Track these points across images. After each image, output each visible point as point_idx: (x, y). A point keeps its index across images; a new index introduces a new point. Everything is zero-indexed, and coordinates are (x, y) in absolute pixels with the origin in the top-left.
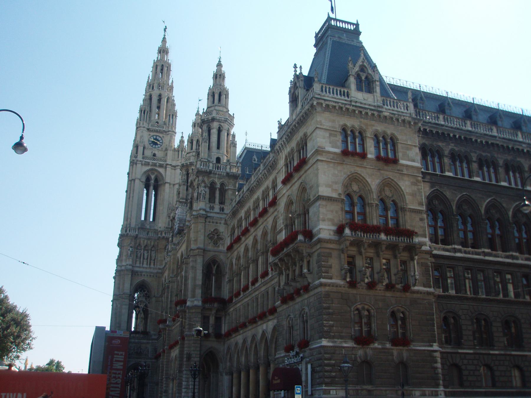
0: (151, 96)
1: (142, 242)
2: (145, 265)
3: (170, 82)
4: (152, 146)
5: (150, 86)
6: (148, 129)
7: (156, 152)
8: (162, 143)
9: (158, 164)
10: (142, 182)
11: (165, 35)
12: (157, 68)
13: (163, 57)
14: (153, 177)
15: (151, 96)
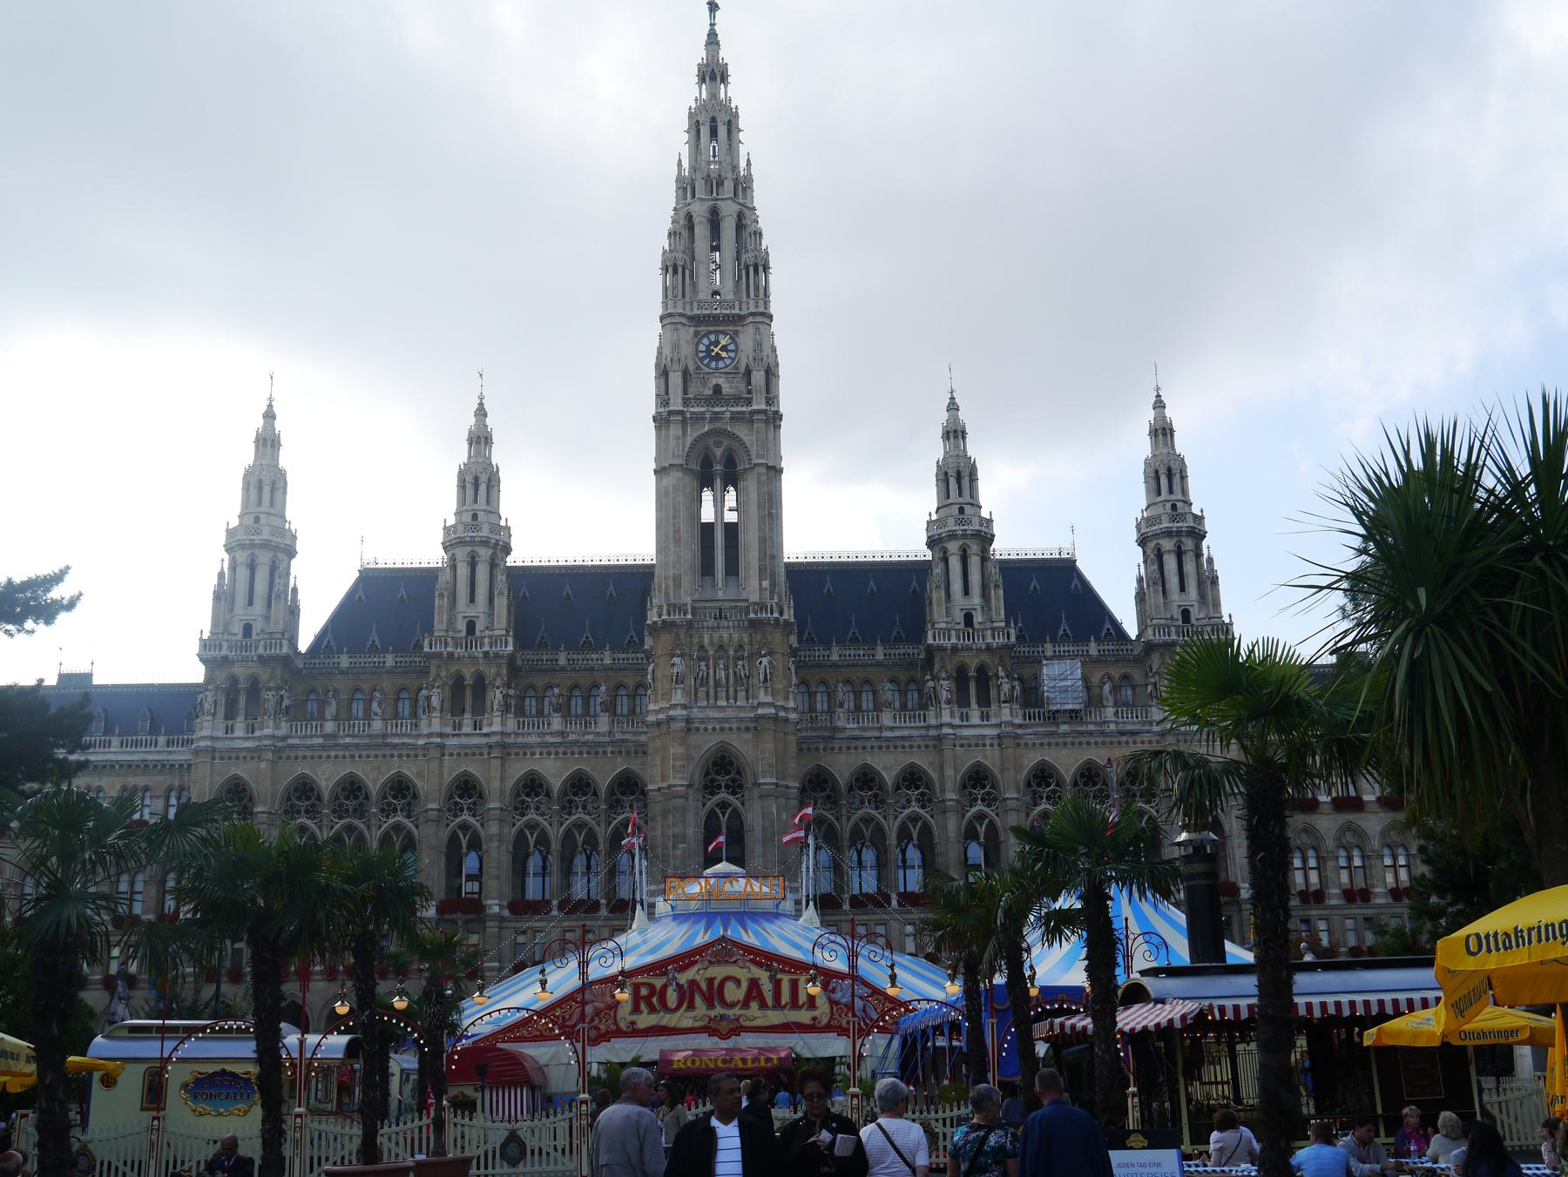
0: (689, 217)
1: (706, 641)
2: (723, 703)
3: (743, 164)
4: (707, 366)
5: (685, 187)
6: (691, 318)
7: (721, 381)
8: (736, 351)
9: (728, 415)
10: (692, 470)
11: (712, 25)
12: (698, 131)
13: (714, 95)
14: (718, 452)
15: (689, 217)
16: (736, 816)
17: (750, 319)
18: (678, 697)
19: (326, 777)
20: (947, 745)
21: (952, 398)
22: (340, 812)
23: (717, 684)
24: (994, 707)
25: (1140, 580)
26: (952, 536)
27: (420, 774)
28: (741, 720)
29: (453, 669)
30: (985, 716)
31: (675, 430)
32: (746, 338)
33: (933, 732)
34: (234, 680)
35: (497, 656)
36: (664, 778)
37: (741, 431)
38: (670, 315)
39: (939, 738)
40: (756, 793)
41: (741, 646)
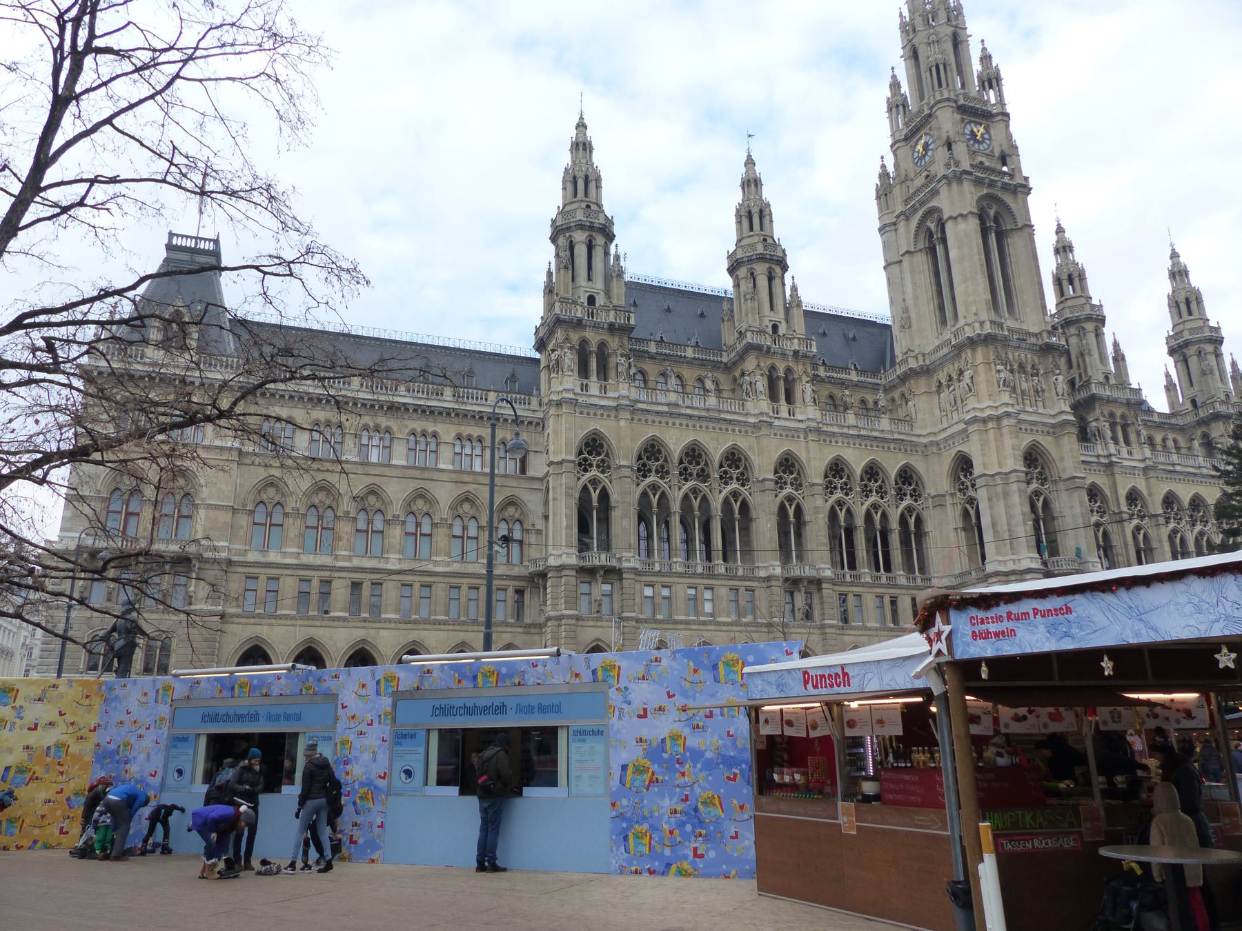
7: (984, 159)
8: (990, 139)
9: (999, 184)
14: (992, 213)
16: (1046, 504)
17: (1000, 118)
18: (1006, 398)
19: (676, 441)
20: (1117, 470)
21: (1059, 225)
22: (685, 475)
23: (1023, 392)
24: (1135, 446)
25: (1168, 375)
26: (1089, 318)
27: (750, 448)
28: (1045, 424)
29: (769, 362)
30: (1130, 453)
31: (967, 186)
32: (997, 131)
33: (1103, 460)
34: (584, 342)
35: (805, 356)
36: (1000, 465)
37: (1008, 198)
38: (948, 100)
39: (1111, 464)
40: (1061, 486)
41: (1033, 367)
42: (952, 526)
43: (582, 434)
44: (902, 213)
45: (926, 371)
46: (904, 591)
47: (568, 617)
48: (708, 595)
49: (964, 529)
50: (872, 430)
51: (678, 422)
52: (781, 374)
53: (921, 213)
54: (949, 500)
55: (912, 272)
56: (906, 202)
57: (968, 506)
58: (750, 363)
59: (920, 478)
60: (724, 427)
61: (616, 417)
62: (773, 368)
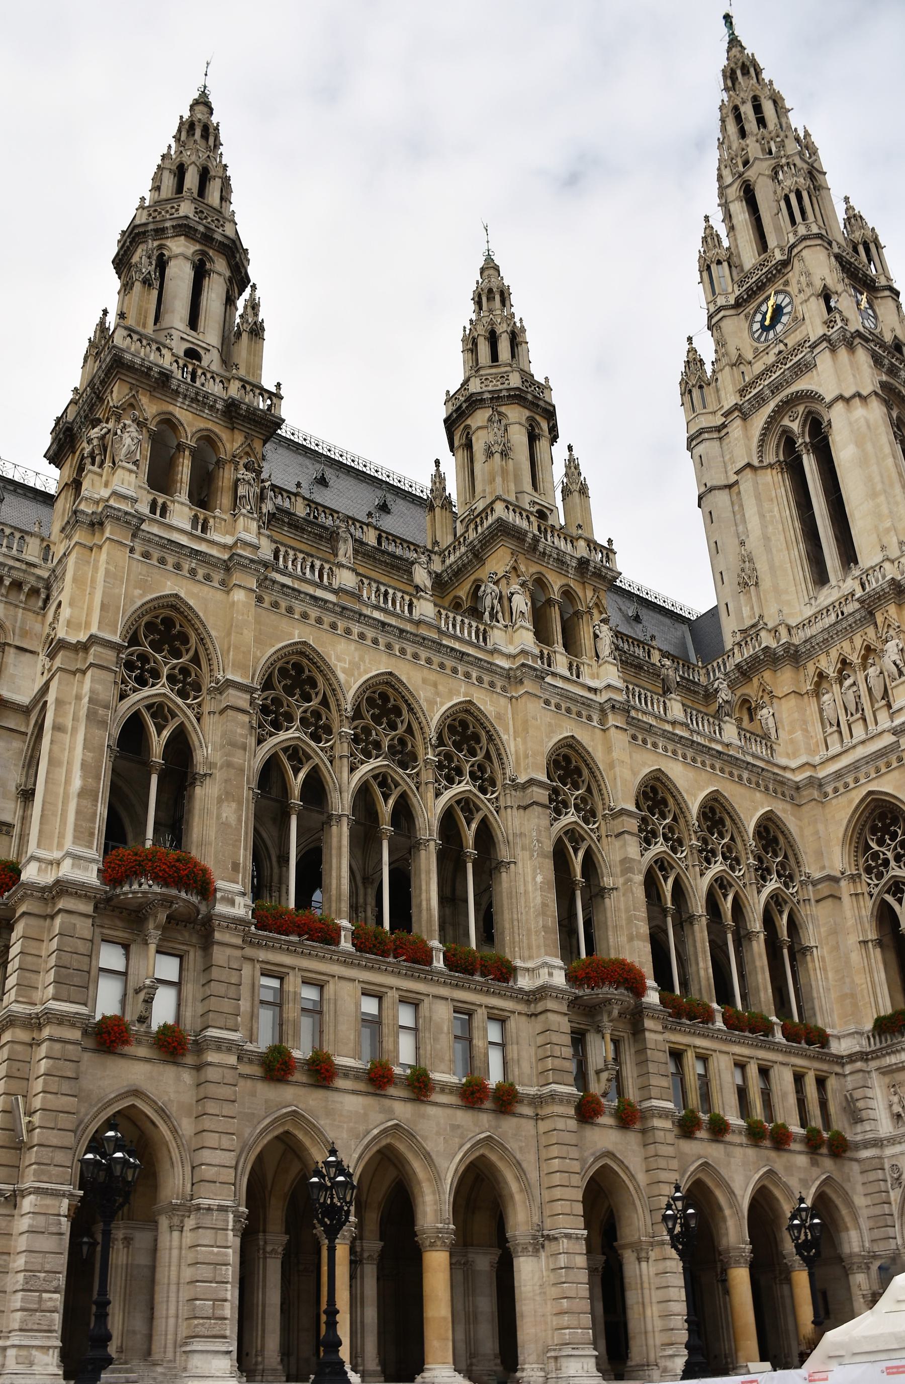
22: (363, 743)
27: (499, 716)
29: (534, 569)
42: (852, 940)
43: (141, 598)
44: (737, 407)
45: (794, 656)
46: (779, 1057)
47: (62, 1020)
48: (406, 1017)
49: (880, 943)
50: (712, 740)
51: (356, 629)
52: (556, 595)
53: (772, 405)
54: (845, 887)
55: (758, 497)
56: (742, 392)
57: (889, 898)
58: (499, 561)
59: (791, 845)
60: (449, 663)
61: (223, 583)
62: (540, 582)
